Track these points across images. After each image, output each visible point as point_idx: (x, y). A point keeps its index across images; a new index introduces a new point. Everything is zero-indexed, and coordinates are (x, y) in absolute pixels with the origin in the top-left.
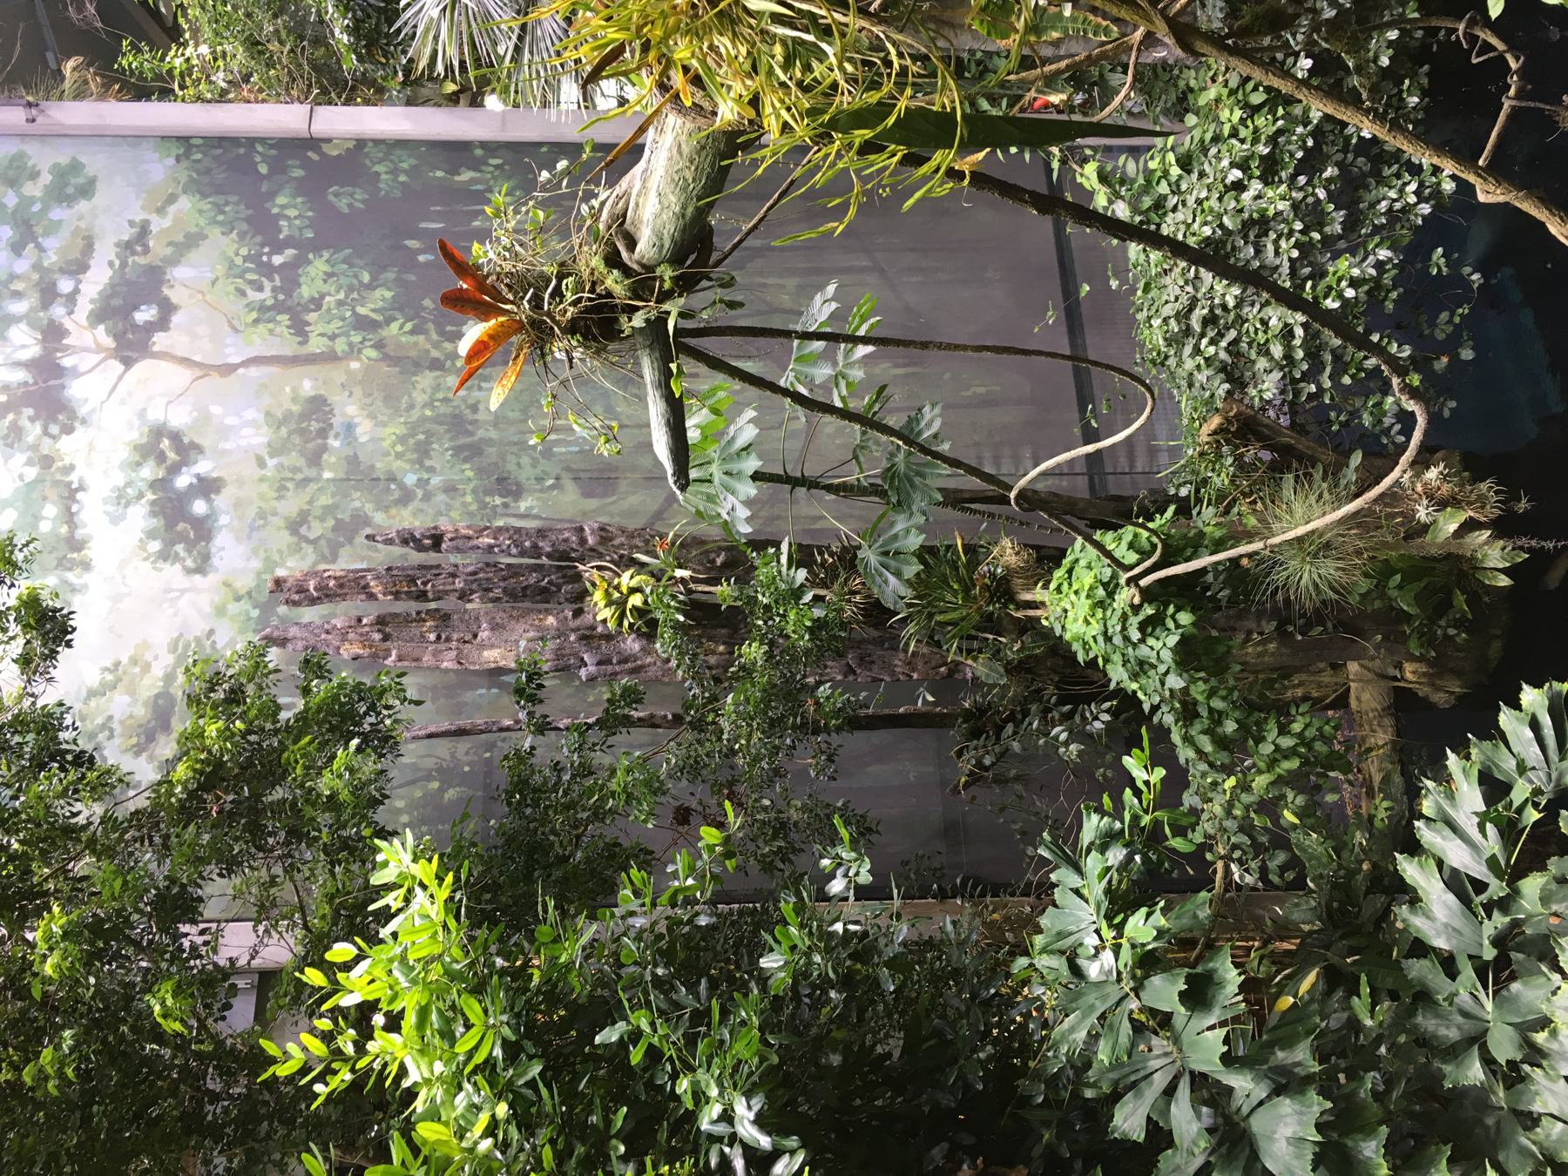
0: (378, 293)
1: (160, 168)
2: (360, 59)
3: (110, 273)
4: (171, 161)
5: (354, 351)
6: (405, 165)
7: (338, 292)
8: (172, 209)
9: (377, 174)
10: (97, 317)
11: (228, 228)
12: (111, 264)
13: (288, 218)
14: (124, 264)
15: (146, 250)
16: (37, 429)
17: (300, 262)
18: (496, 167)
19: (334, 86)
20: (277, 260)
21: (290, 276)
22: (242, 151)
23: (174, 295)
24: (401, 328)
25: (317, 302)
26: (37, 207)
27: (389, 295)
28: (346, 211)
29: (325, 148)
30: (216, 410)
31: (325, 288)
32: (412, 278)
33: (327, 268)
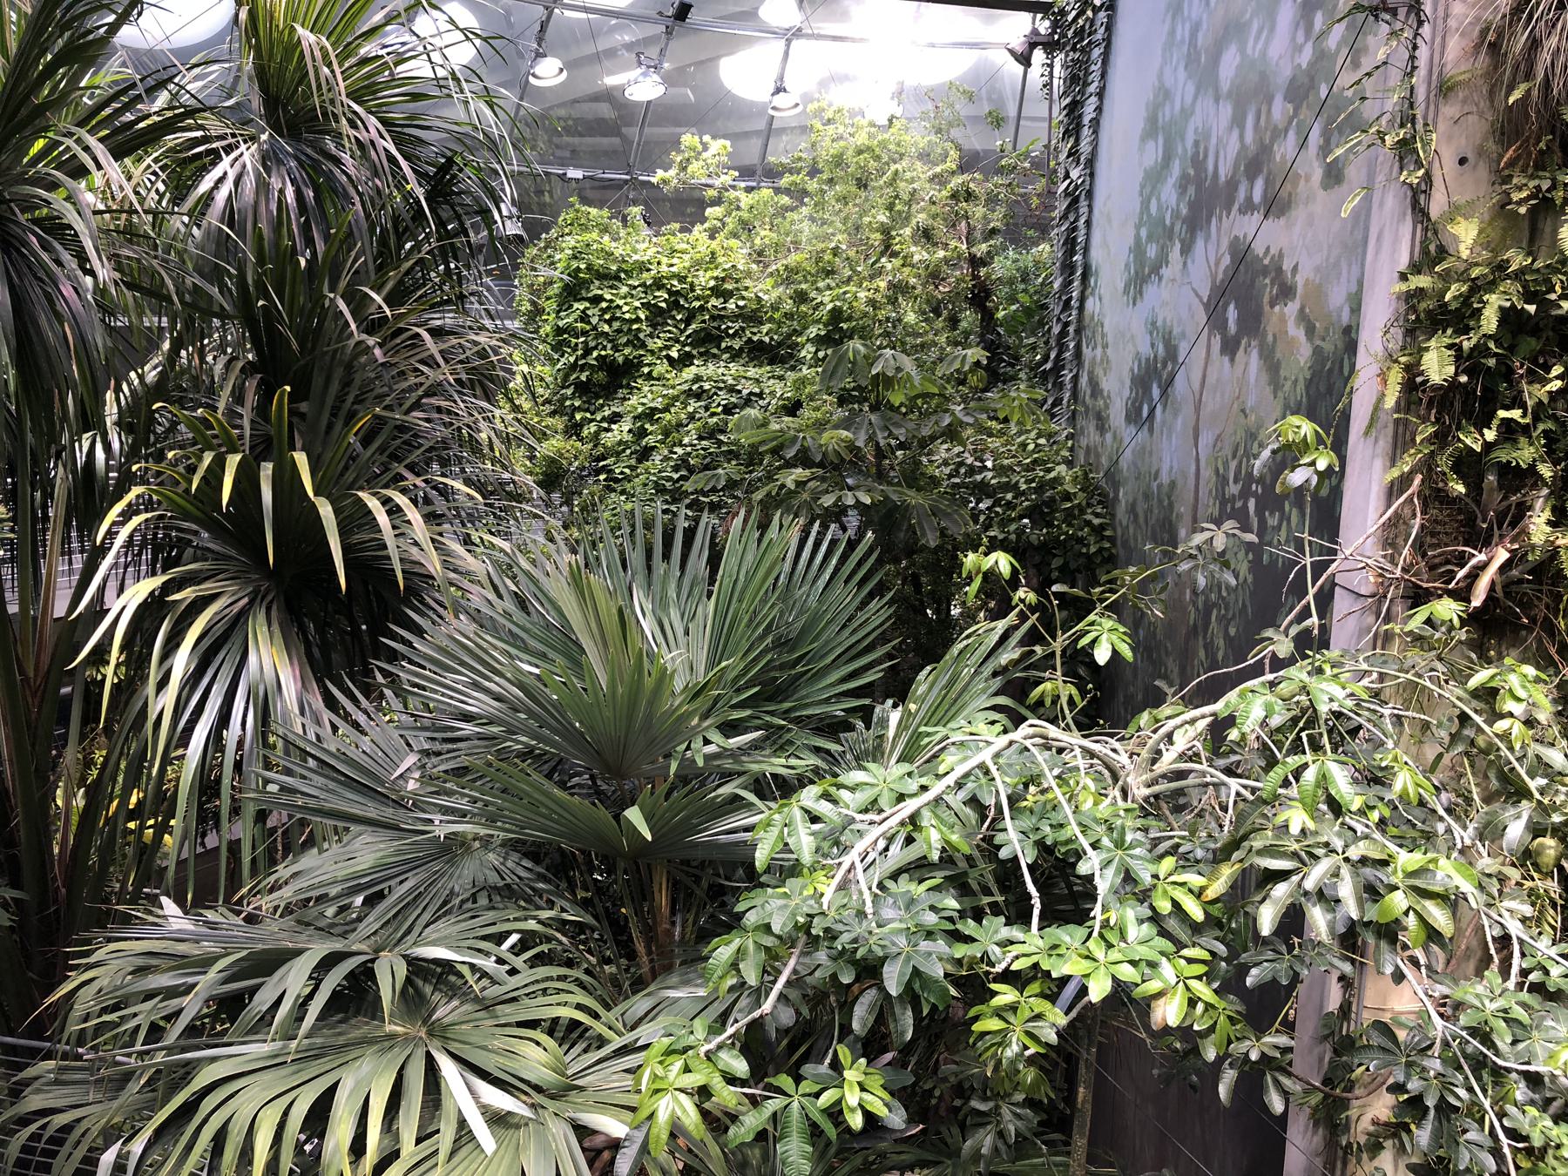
13: (1279, 527)
14: (1265, 271)
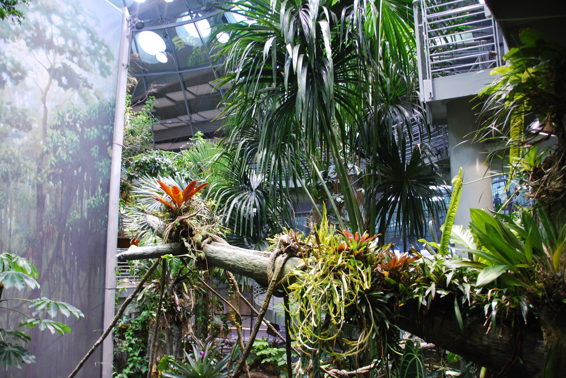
0: (65, 155)
1: (107, 97)
2: (136, 163)
3: (78, 73)
4: (109, 101)
5: (46, 143)
6: (104, 171)
7: (67, 142)
8: (95, 97)
9: (101, 162)
10: (64, 65)
11: (89, 113)
12: (81, 75)
13: (90, 132)
14: (80, 78)
15: (83, 86)
17: (77, 133)
18: (102, 200)
19: (128, 153)
20: (78, 125)
21: (73, 128)
22: (110, 122)
23: (70, 91)
24: (53, 161)
25: (64, 135)
26: (99, 58)
27: (64, 158)
28: (92, 150)
29: (110, 147)
30: (30, 93)
31: (68, 138)
32: (69, 167)
33: (74, 140)
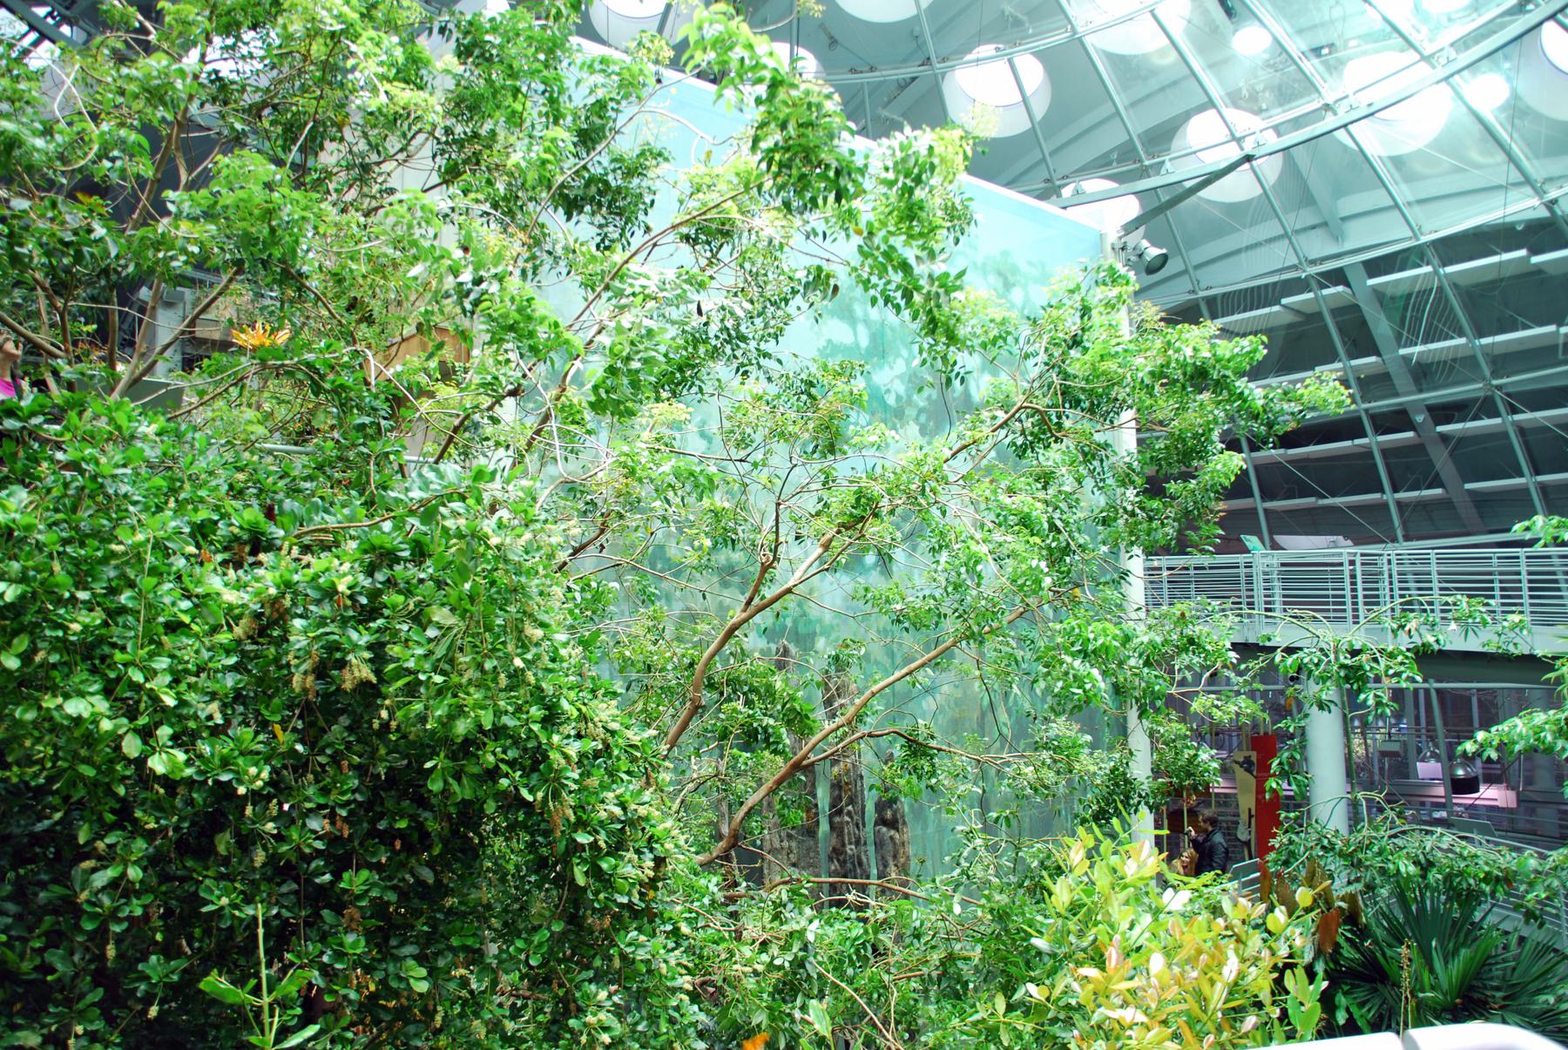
16: (922, 404)
